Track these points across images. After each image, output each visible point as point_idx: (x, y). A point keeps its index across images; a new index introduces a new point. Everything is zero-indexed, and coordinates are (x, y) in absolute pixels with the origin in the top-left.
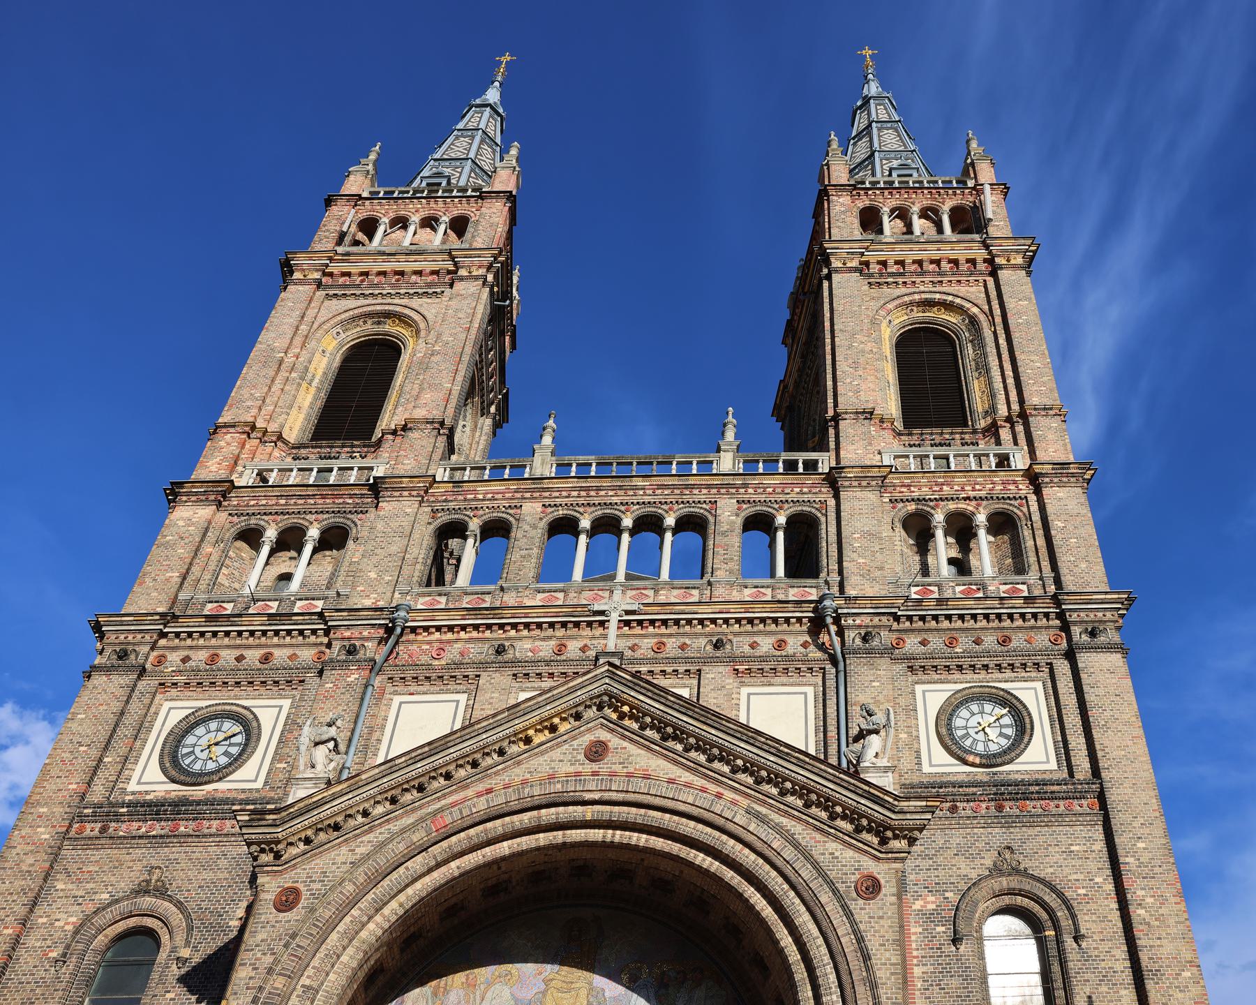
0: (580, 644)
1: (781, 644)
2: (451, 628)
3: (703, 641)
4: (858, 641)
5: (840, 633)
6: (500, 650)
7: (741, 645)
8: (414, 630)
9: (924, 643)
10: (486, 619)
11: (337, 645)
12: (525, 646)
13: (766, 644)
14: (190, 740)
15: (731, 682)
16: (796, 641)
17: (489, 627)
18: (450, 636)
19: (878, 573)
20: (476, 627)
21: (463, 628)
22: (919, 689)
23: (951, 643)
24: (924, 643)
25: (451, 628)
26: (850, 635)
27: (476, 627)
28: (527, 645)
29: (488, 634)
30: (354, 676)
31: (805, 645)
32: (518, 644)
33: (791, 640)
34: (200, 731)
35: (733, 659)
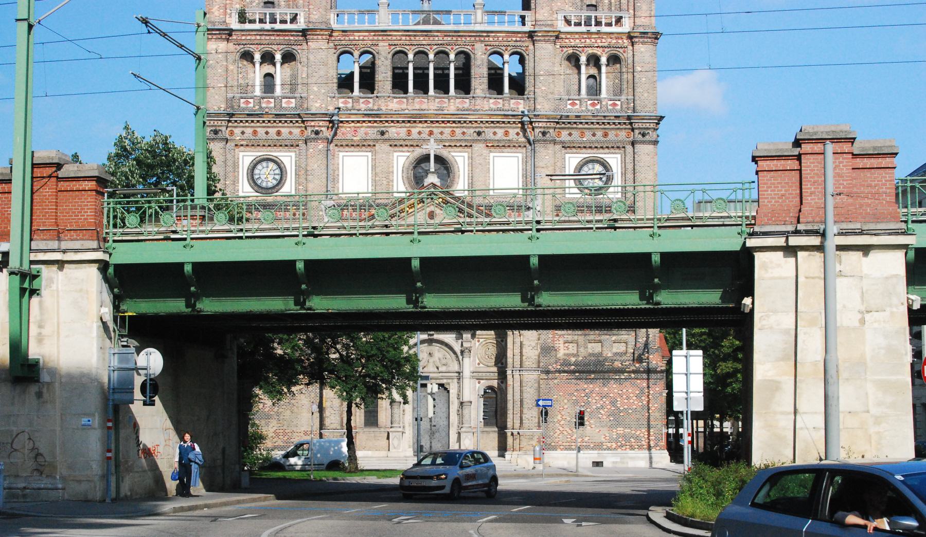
0: (417, 130)
1: (506, 133)
2: (358, 122)
3: (472, 130)
4: (540, 135)
5: (533, 129)
6: (383, 133)
7: (489, 133)
8: (342, 122)
9: (570, 134)
10: (374, 117)
11: (309, 129)
12: (394, 131)
13: (500, 132)
14: (256, 171)
15: (485, 151)
16: (514, 133)
17: (375, 122)
18: (358, 125)
19: (550, 96)
20: (370, 122)
21: (364, 121)
22: (567, 156)
23: (582, 135)
24: (570, 134)
25: (358, 122)
26: (537, 130)
27: (370, 122)
28: (394, 130)
29: (375, 124)
30: (321, 146)
31: (518, 134)
32: (390, 130)
33: (511, 131)
34: (259, 167)
35: (486, 140)
